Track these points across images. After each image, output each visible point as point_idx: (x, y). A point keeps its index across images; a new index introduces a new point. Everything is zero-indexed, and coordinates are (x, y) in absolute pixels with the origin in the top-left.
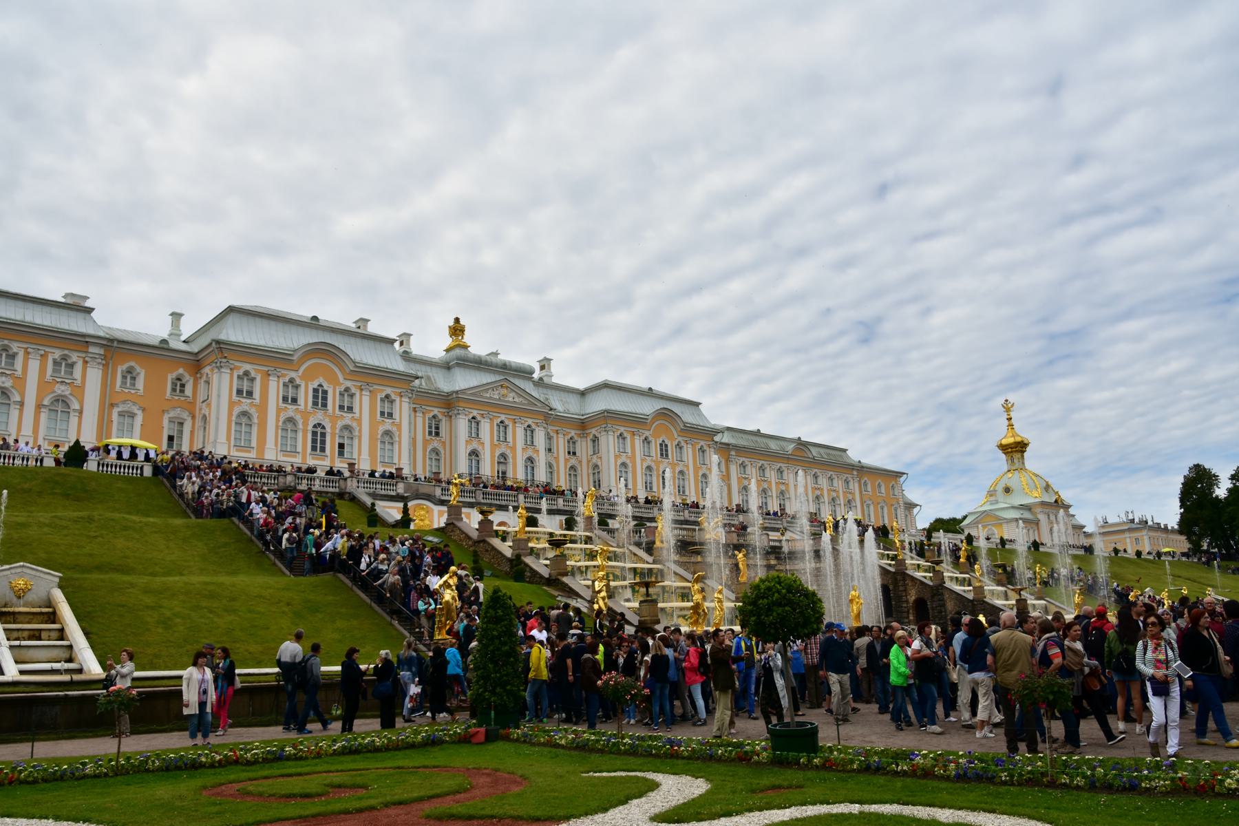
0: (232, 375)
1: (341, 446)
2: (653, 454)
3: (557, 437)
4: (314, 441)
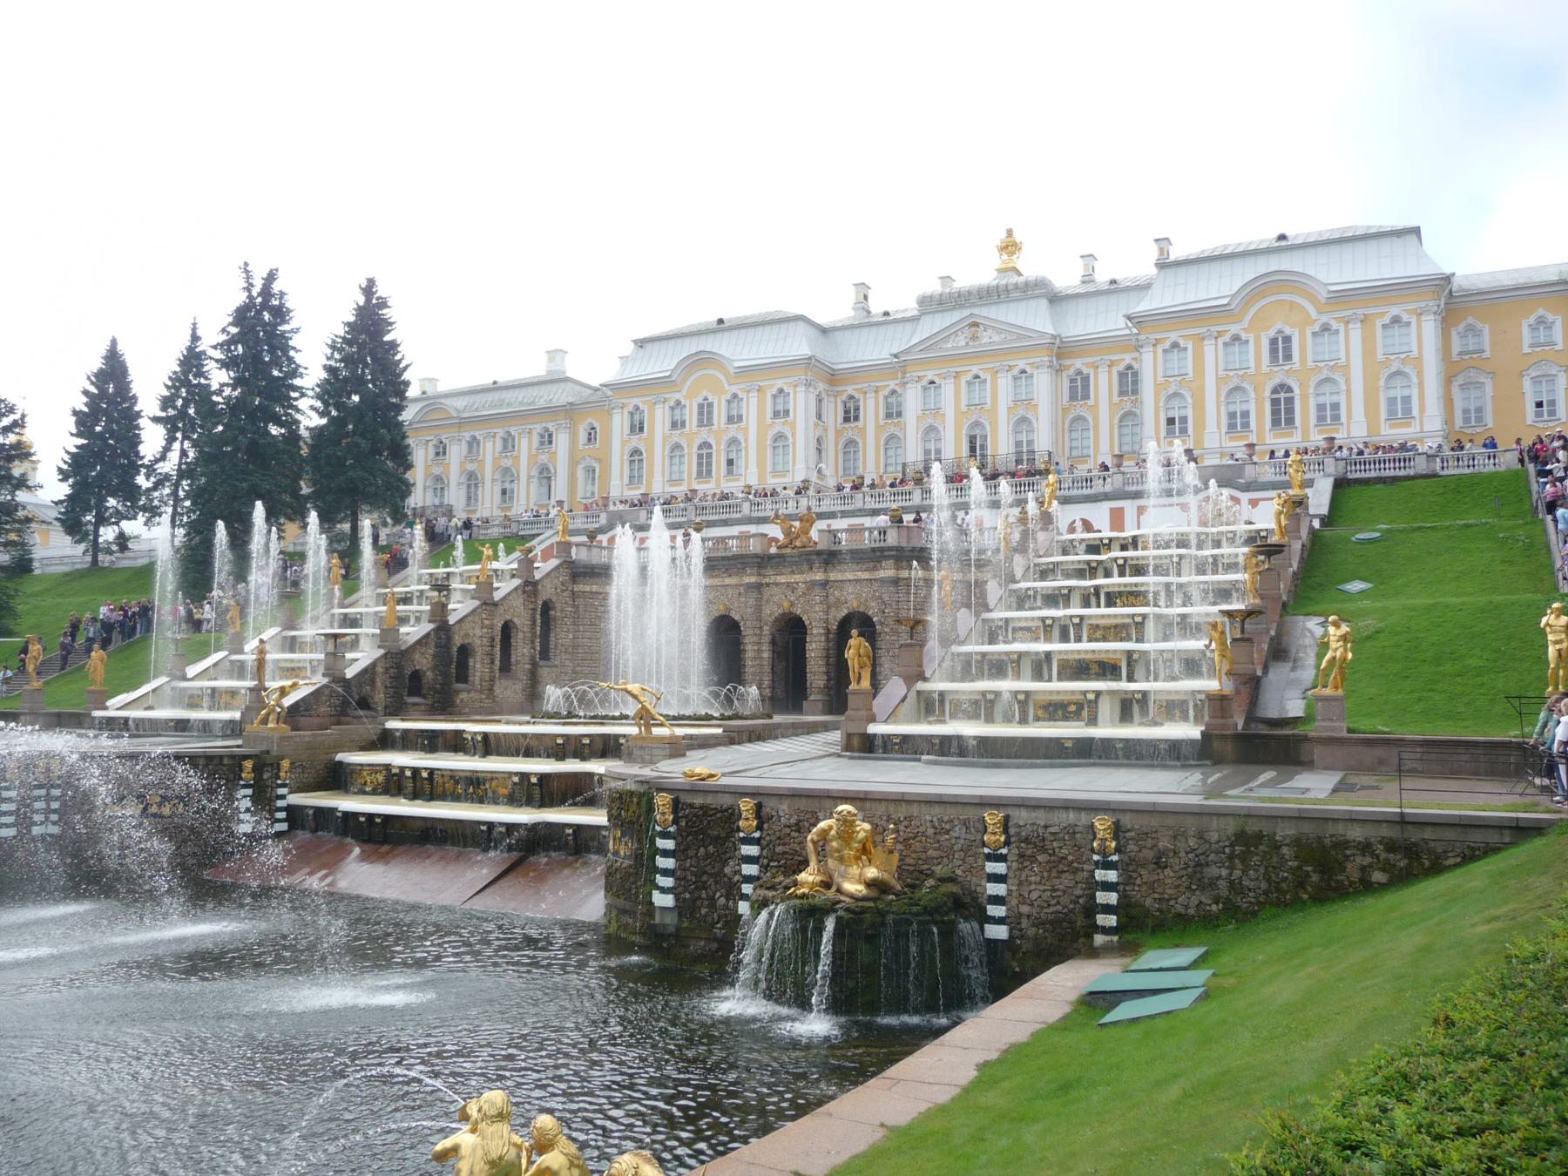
1: (730, 462)
3: (1096, 374)
4: (700, 465)
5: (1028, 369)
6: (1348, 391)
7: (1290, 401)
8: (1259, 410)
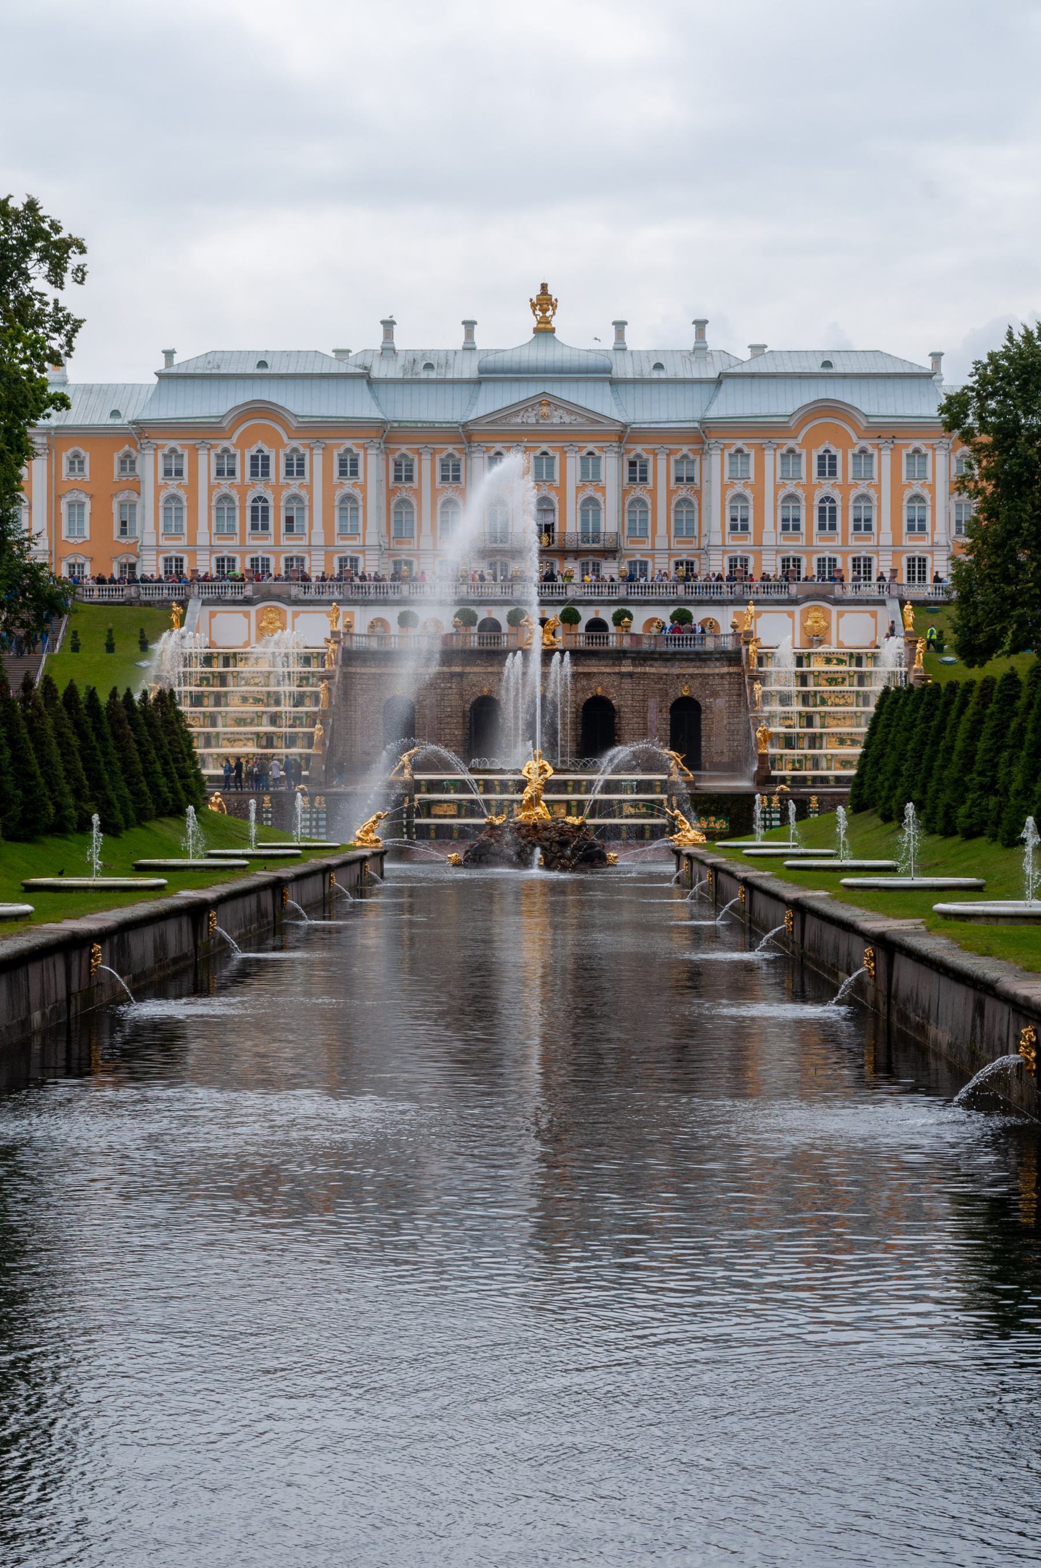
0: (156, 456)
1: (289, 520)
2: (804, 474)
4: (254, 518)
5: (597, 453)
6: (879, 507)
7: (833, 510)
8: (808, 517)
